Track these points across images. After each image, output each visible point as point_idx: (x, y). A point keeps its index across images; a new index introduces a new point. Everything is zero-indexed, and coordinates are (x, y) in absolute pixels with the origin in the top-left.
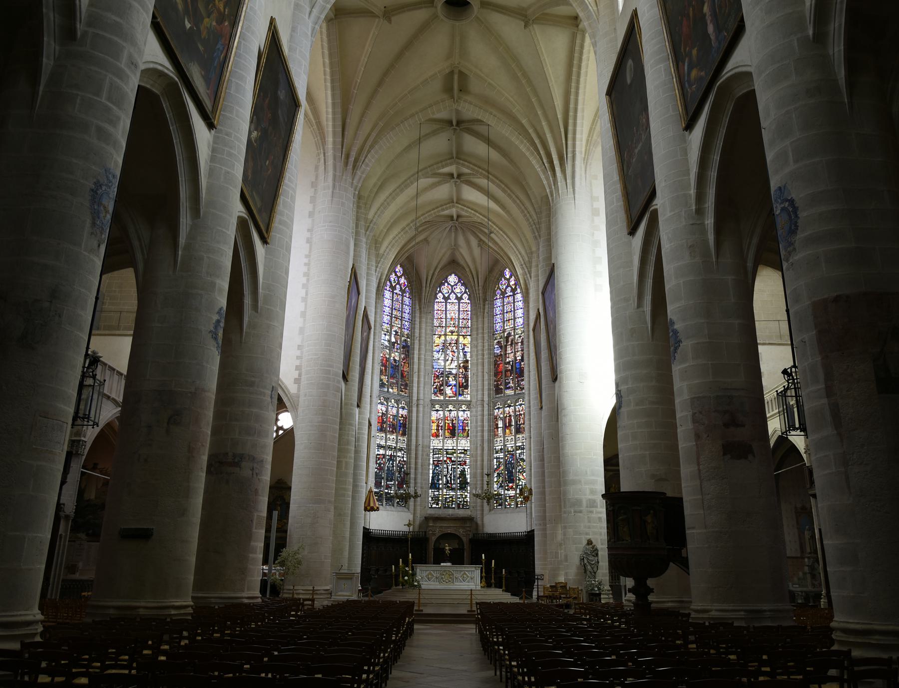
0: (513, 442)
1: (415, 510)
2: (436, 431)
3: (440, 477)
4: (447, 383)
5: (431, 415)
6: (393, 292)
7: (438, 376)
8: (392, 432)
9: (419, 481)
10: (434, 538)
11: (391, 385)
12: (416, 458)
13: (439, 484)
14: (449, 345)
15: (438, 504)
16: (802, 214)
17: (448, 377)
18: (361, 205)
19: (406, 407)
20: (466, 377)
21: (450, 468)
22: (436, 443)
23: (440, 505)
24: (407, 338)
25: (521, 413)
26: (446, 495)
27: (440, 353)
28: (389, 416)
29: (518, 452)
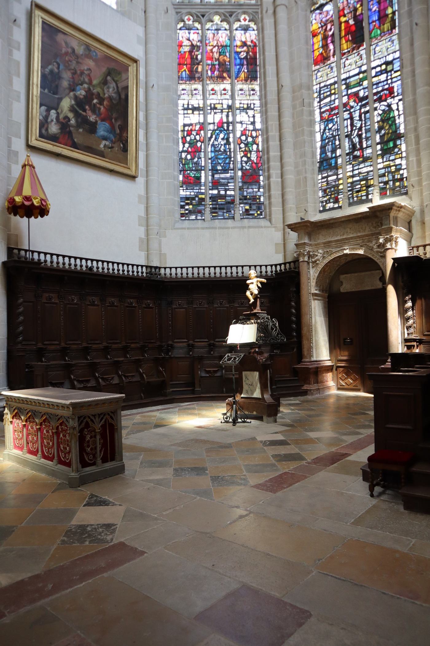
2: (321, 50)
8: (221, 78)
15: (336, 201)
19: (252, 25)
21: (356, 115)
23: (341, 202)
26: (353, 176)
28: (209, 48)
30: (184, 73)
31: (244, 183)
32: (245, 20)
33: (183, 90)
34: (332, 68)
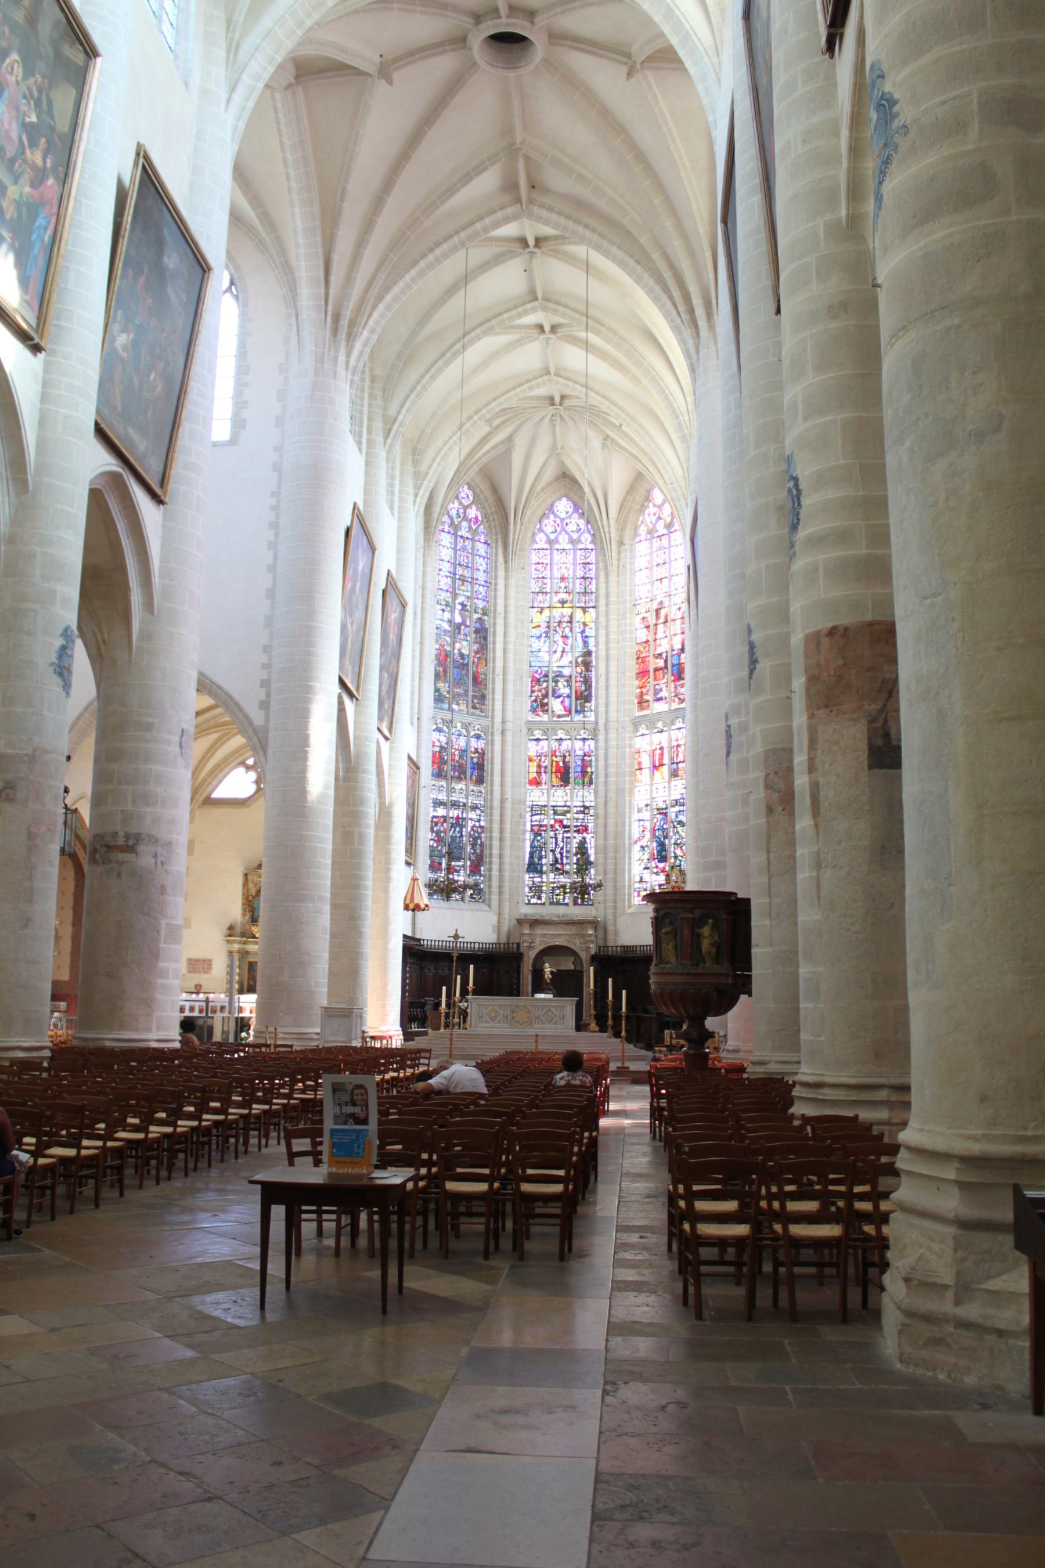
0: (667, 794)
1: (500, 907)
2: (535, 775)
3: (543, 853)
4: (554, 691)
5: (527, 748)
6: (455, 535)
7: (538, 680)
8: (459, 779)
9: (507, 859)
10: (532, 954)
11: (456, 698)
12: (502, 822)
13: (542, 865)
14: (559, 625)
15: (539, 898)
16: (806, 501)
17: (556, 682)
18: (376, 392)
20: (587, 682)
21: (560, 837)
22: (537, 796)
23: (543, 900)
24: (485, 614)
25: (681, 742)
26: (554, 883)
27: (543, 639)
29: (677, 808)
31: (471, 871)
32: (478, 730)
34: (543, 793)
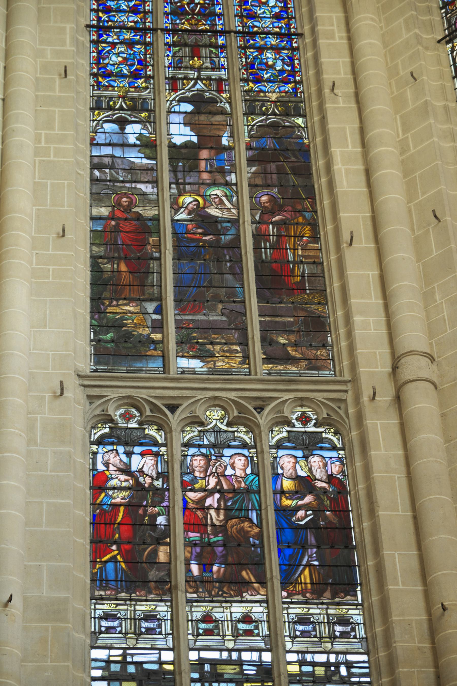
30: (110, 566)
32: (304, 420)
33: (107, 617)
